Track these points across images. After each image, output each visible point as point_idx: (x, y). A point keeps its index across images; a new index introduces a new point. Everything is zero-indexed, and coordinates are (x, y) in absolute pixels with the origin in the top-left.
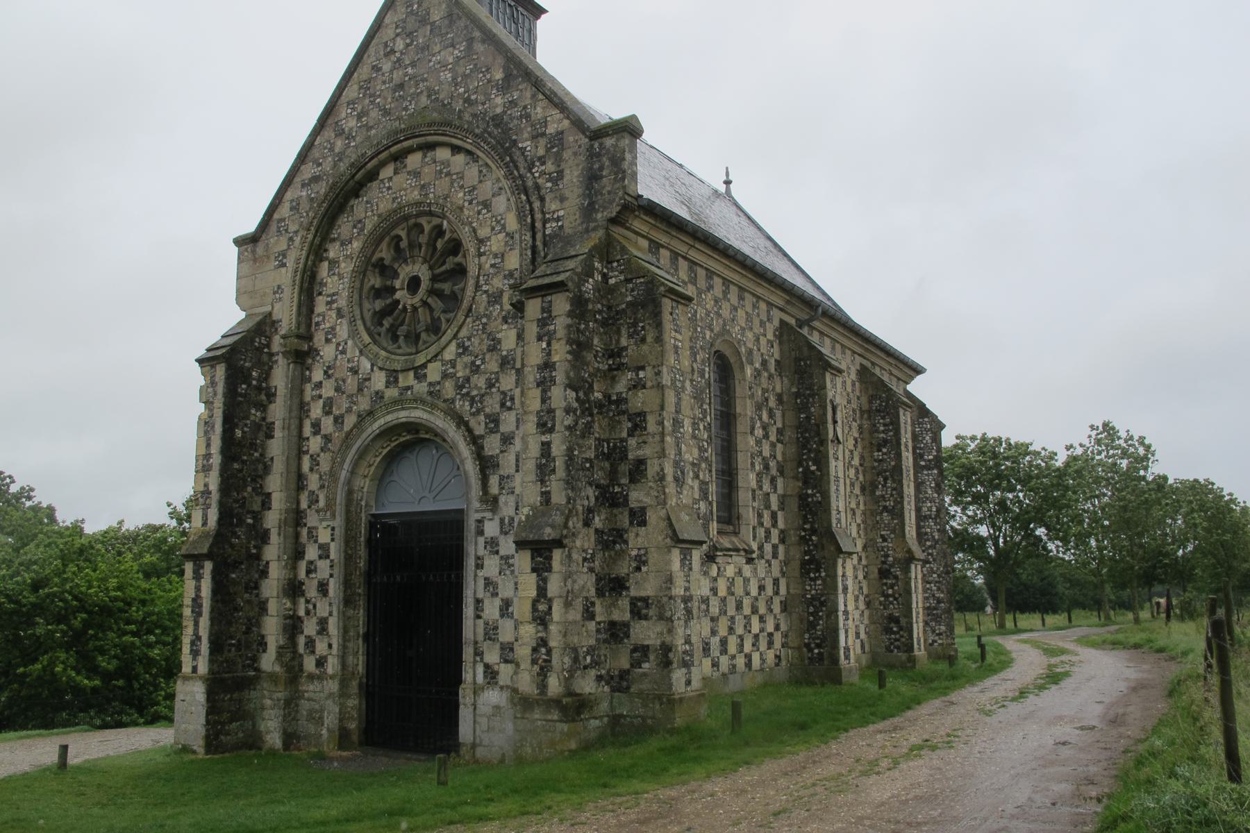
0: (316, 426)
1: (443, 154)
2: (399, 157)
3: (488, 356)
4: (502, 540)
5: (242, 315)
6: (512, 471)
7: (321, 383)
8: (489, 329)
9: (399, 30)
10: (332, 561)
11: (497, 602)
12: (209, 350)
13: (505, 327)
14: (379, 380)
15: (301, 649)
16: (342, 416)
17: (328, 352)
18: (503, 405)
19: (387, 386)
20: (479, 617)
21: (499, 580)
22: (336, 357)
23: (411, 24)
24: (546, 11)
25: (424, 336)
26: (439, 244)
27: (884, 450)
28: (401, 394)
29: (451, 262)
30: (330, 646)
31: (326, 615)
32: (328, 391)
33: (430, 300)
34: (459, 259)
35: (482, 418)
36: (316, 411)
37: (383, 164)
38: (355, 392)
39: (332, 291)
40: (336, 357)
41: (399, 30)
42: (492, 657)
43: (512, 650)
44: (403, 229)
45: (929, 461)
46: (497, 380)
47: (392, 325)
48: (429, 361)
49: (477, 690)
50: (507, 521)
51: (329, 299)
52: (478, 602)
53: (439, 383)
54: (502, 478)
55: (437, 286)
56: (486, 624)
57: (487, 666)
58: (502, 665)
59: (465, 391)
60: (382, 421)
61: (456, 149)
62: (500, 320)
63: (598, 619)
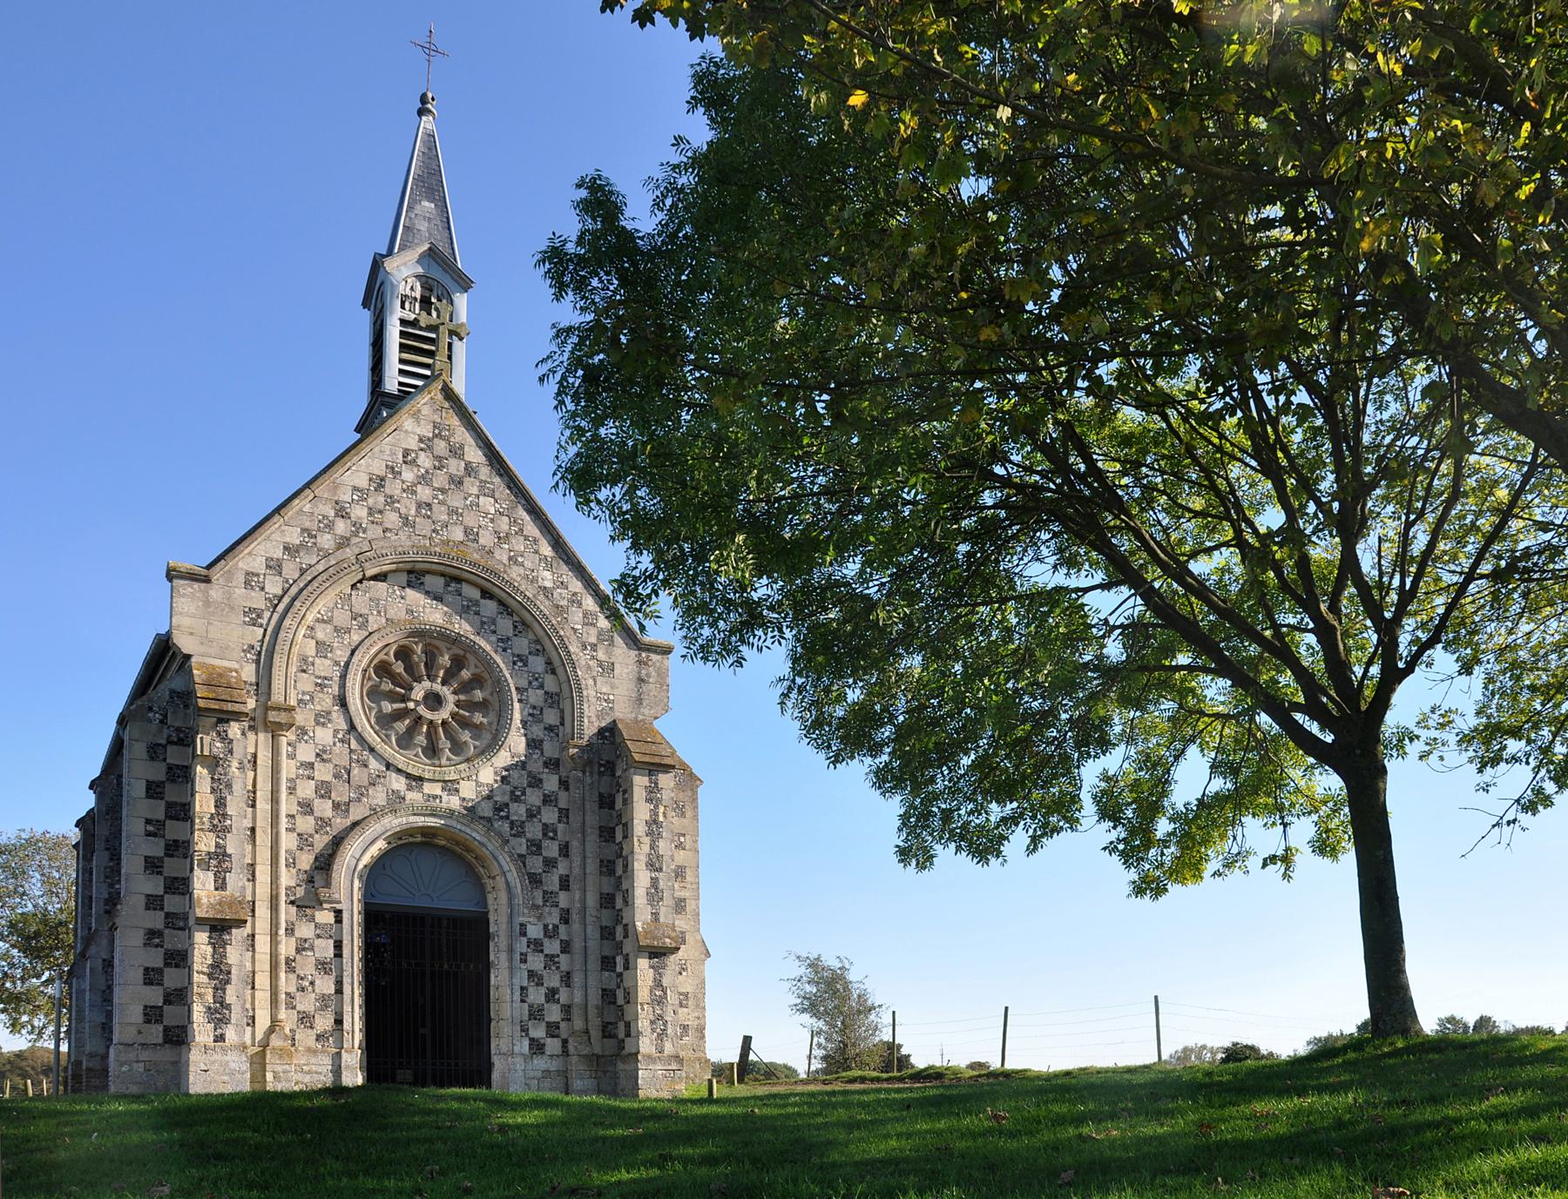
3: (529, 791)
4: (546, 942)
6: (556, 888)
8: (529, 768)
13: (546, 770)
18: (545, 835)
19: (410, 788)
21: (545, 973)
22: (334, 744)
23: (441, 447)
32: (323, 773)
35: (524, 841)
38: (366, 784)
39: (323, 674)
40: (334, 744)
43: (558, 1028)
46: (539, 813)
50: (550, 927)
52: (522, 988)
54: (545, 892)
57: (532, 1040)
58: (549, 1040)
60: (404, 820)
62: (540, 763)
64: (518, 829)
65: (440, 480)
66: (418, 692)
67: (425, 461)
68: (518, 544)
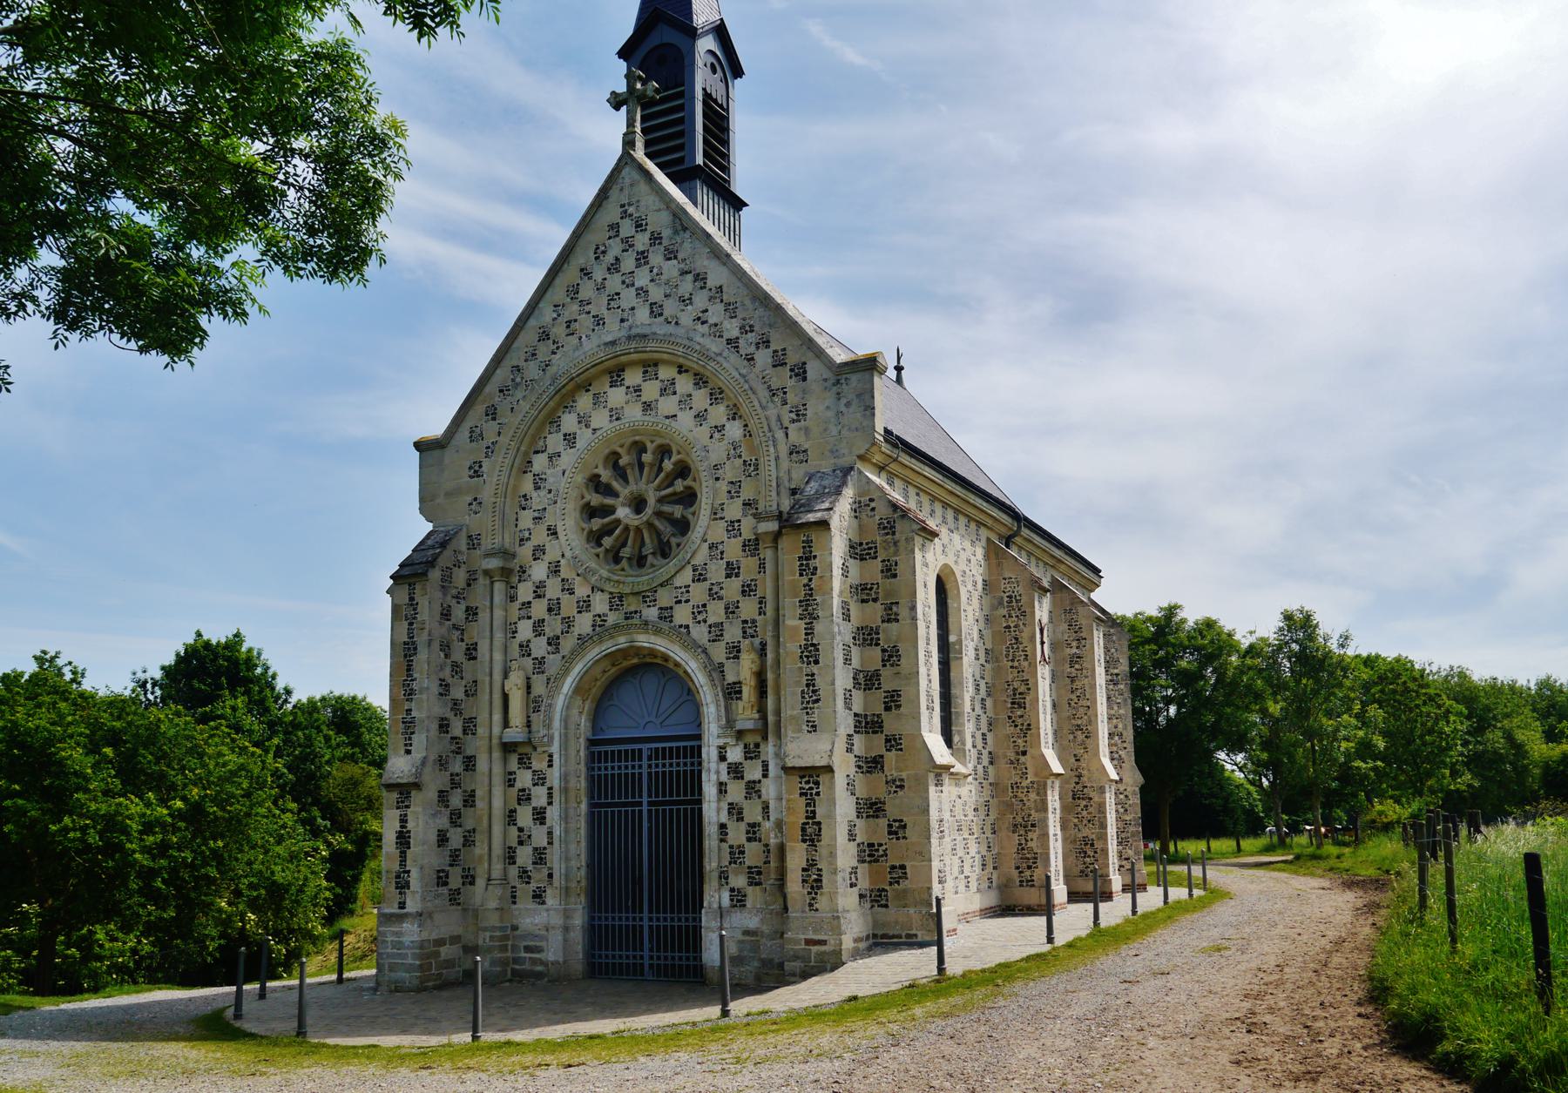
0: (525, 648)
1: (665, 373)
2: (616, 374)
5: (429, 527)
7: (529, 603)
9: (612, 233)
10: (550, 788)
11: (743, 826)
12: (402, 566)
14: (600, 604)
15: (515, 881)
16: (558, 638)
17: (539, 571)
20: (722, 840)
23: (627, 228)
24: (746, 205)
25: (650, 558)
26: (668, 465)
27: (1077, 666)
28: (627, 618)
29: (679, 485)
30: (550, 876)
31: (545, 843)
33: (657, 523)
34: (689, 482)
36: (525, 630)
37: (597, 376)
41: (612, 233)
42: (739, 881)
44: (622, 446)
45: (1117, 675)
47: (613, 547)
48: (661, 585)
49: (721, 912)
51: (536, 514)
52: (723, 826)
53: (671, 608)
55: (667, 508)
56: (731, 847)
59: (700, 618)
61: (681, 370)
63: (859, 840)
64: (717, 632)
65: (629, 263)
66: (623, 513)
67: (615, 248)
68: (701, 300)
